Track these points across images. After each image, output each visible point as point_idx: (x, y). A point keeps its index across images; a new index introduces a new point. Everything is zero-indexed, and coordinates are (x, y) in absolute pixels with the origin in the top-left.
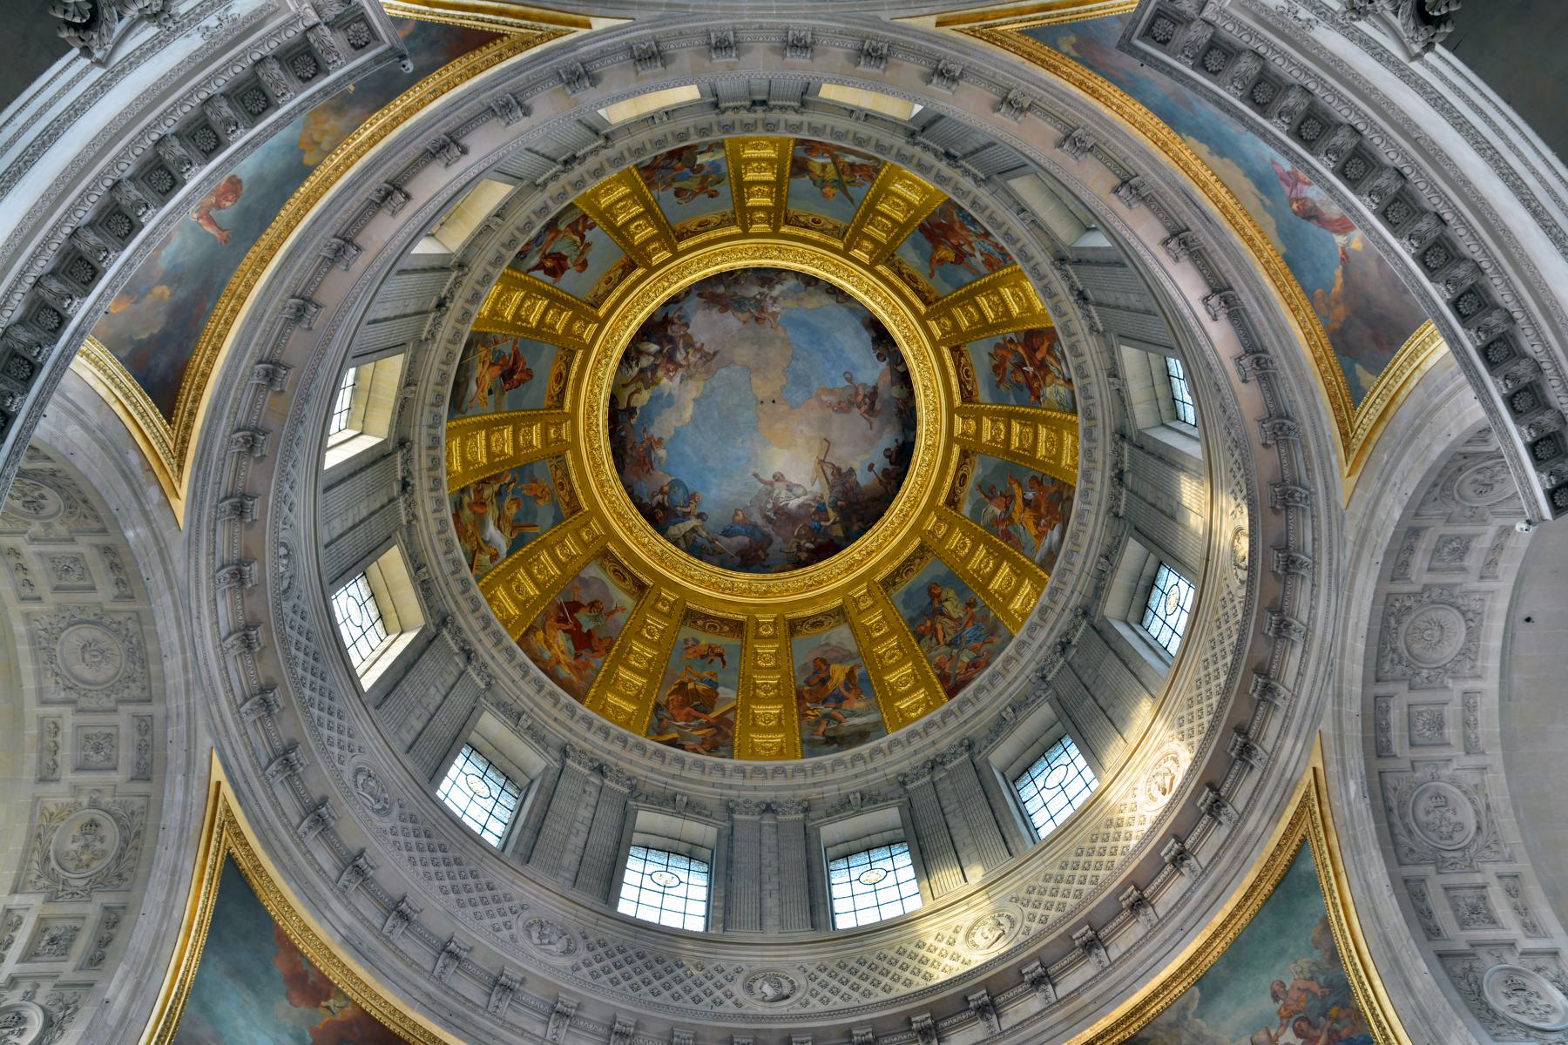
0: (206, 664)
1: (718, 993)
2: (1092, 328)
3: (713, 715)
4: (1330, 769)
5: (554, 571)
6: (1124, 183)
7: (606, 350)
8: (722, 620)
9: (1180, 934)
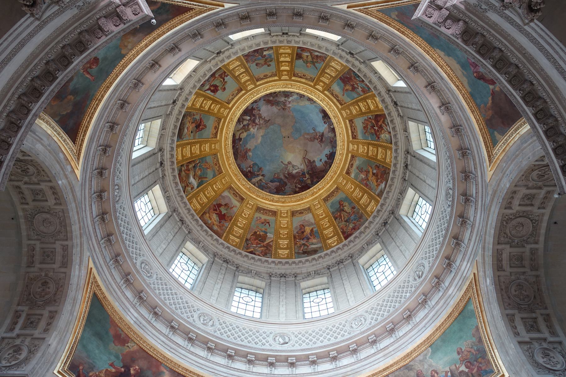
0: (88, 227)
1: (264, 341)
2: (399, 115)
3: (265, 243)
4: (480, 274)
5: (213, 194)
6: (412, 65)
7: (232, 119)
8: (269, 211)
9: (425, 328)
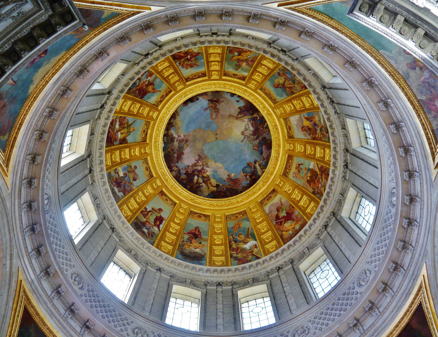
7: (191, 199)
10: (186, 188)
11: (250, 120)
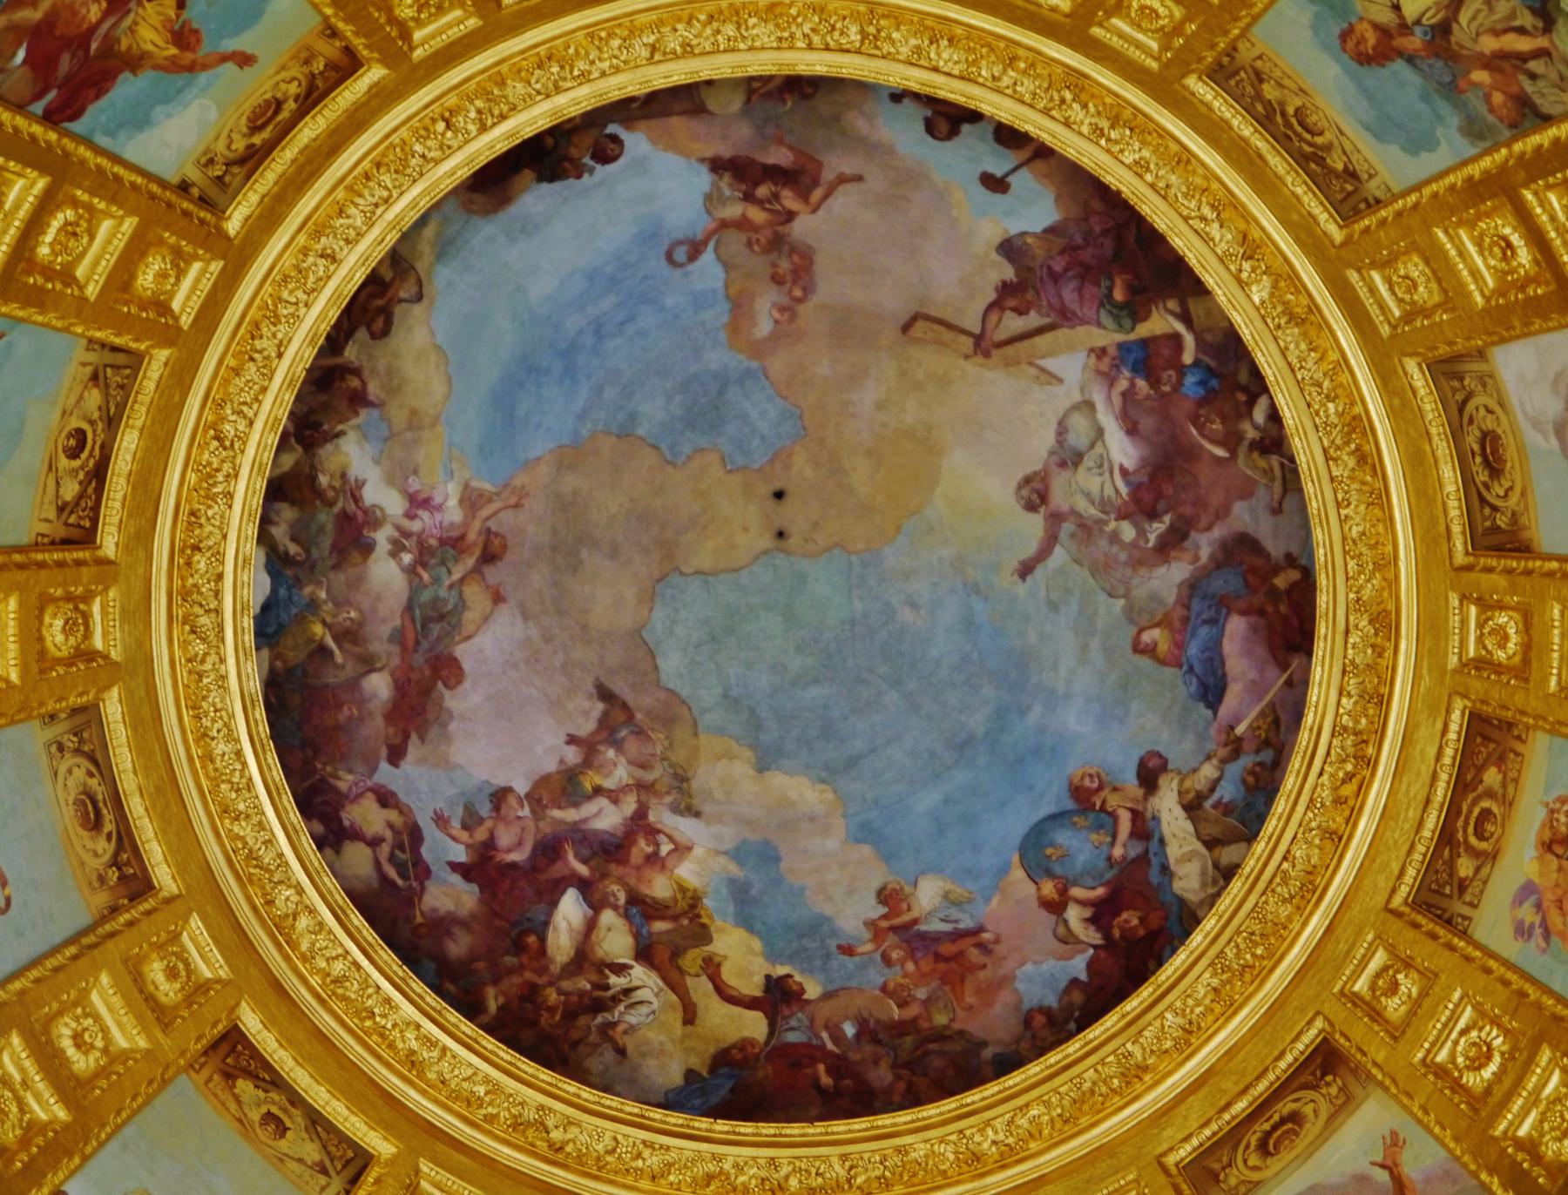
7: (518, 1125)
8: (1464, 785)
10: (471, 1008)
11: (1108, 364)
